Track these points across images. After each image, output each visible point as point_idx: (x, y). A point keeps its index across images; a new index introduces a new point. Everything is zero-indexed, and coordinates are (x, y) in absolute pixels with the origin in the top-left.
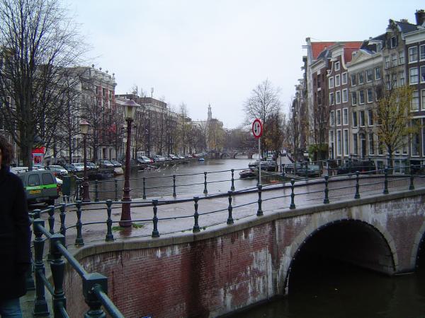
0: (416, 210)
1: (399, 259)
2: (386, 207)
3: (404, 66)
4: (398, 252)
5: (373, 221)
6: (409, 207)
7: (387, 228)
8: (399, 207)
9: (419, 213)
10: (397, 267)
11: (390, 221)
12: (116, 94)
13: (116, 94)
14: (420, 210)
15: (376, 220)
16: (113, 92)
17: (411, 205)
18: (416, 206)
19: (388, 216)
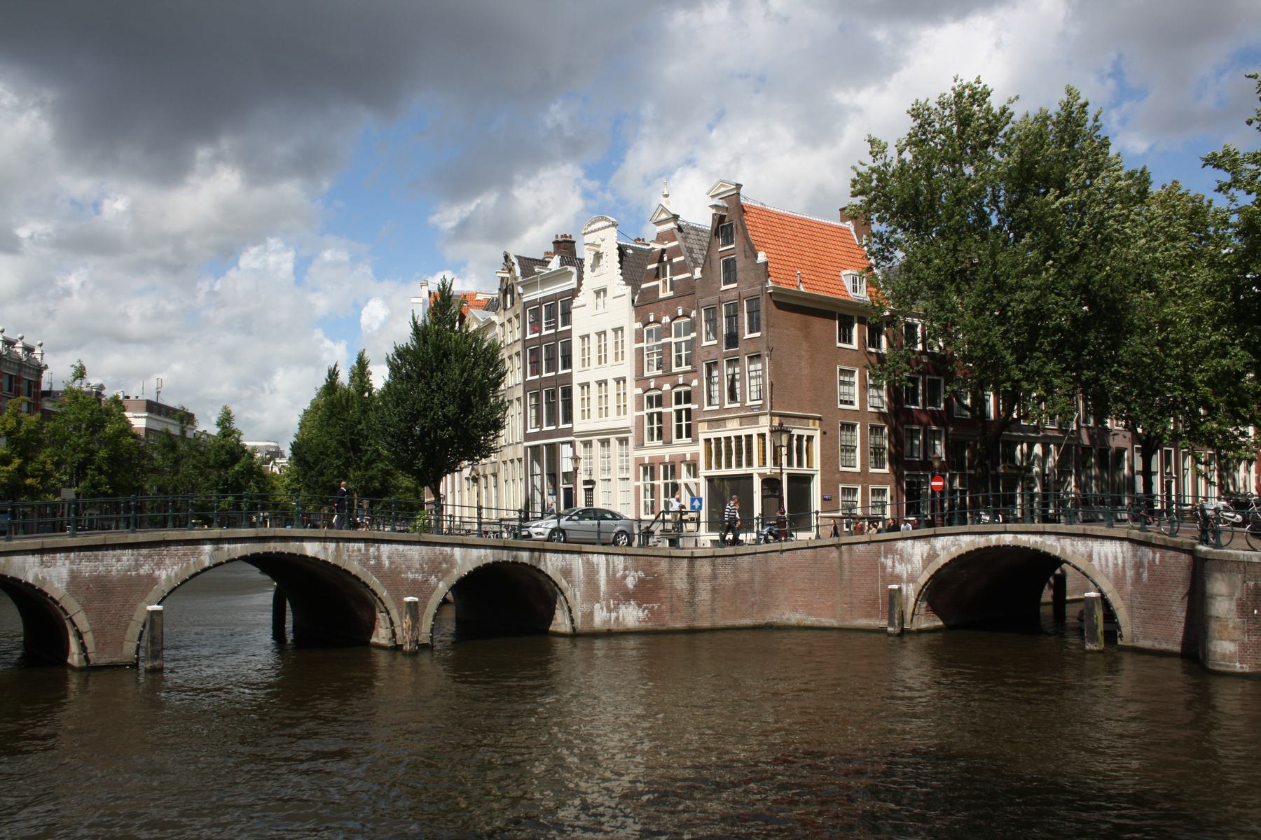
0: (137, 566)
1: (97, 644)
2: (67, 558)
3: (520, 343)
4: (93, 631)
5: (36, 577)
6: (119, 560)
7: (68, 590)
8: (96, 558)
9: (142, 572)
10: (91, 656)
11: (74, 578)
12: (45, 387)
13: (45, 387)
14: (146, 567)
15: (44, 578)
16: (38, 384)
17: (125, 558)
18: (137, 560)
19: (72, 571)
